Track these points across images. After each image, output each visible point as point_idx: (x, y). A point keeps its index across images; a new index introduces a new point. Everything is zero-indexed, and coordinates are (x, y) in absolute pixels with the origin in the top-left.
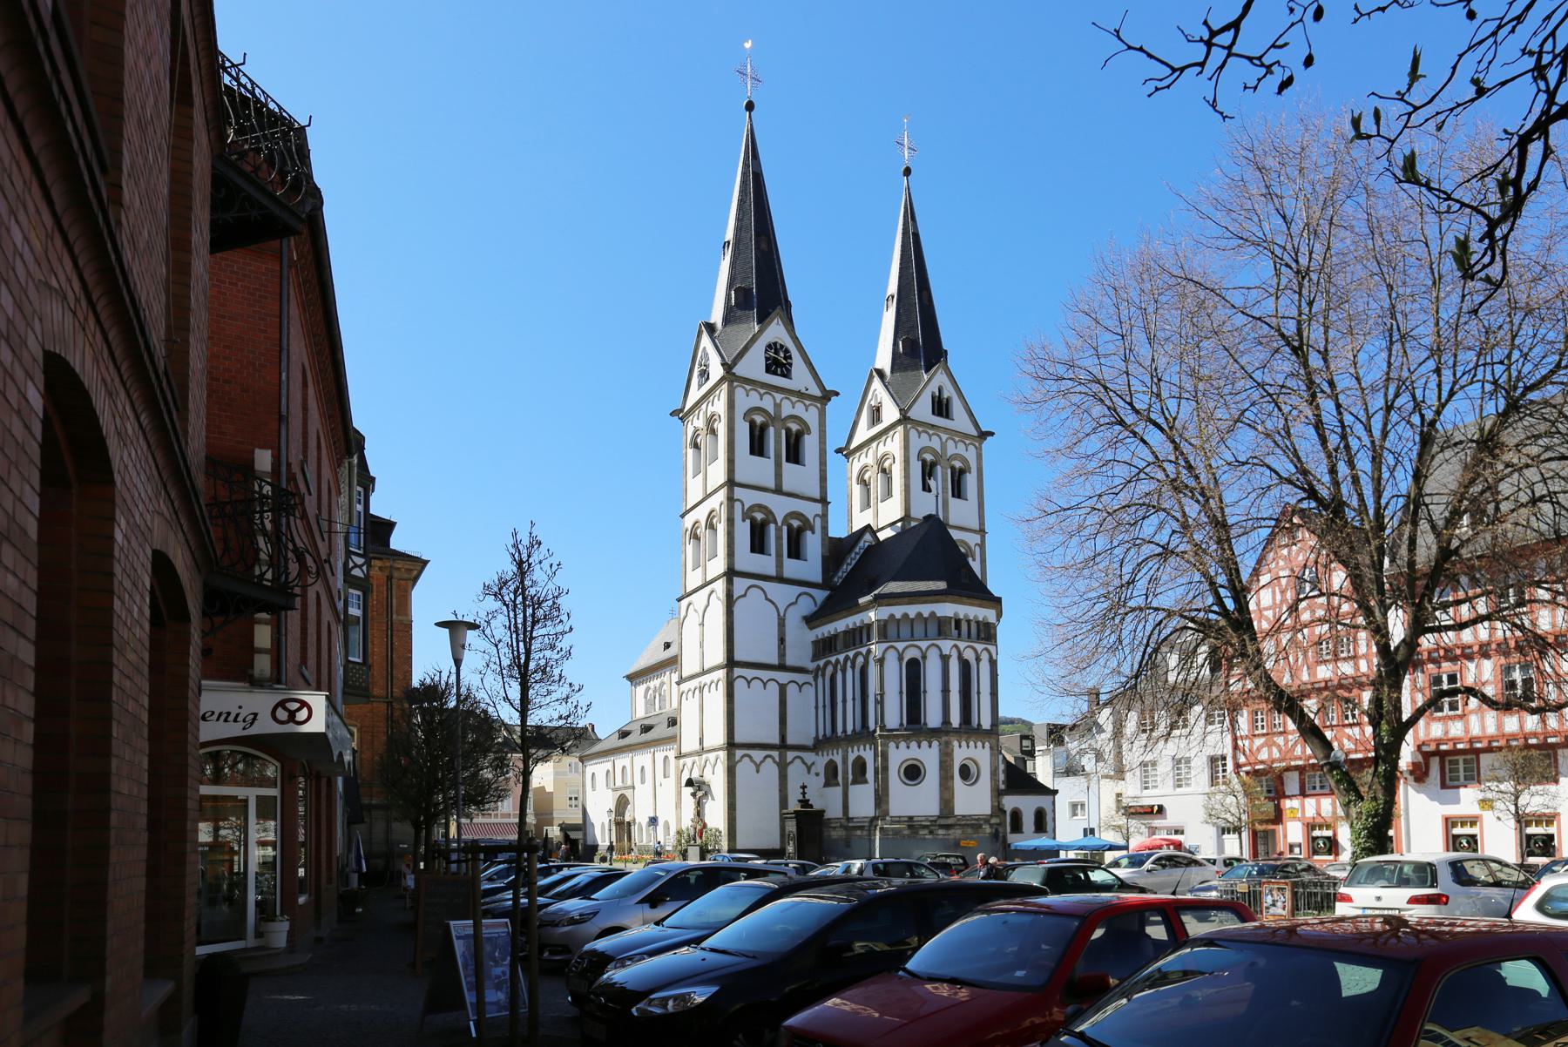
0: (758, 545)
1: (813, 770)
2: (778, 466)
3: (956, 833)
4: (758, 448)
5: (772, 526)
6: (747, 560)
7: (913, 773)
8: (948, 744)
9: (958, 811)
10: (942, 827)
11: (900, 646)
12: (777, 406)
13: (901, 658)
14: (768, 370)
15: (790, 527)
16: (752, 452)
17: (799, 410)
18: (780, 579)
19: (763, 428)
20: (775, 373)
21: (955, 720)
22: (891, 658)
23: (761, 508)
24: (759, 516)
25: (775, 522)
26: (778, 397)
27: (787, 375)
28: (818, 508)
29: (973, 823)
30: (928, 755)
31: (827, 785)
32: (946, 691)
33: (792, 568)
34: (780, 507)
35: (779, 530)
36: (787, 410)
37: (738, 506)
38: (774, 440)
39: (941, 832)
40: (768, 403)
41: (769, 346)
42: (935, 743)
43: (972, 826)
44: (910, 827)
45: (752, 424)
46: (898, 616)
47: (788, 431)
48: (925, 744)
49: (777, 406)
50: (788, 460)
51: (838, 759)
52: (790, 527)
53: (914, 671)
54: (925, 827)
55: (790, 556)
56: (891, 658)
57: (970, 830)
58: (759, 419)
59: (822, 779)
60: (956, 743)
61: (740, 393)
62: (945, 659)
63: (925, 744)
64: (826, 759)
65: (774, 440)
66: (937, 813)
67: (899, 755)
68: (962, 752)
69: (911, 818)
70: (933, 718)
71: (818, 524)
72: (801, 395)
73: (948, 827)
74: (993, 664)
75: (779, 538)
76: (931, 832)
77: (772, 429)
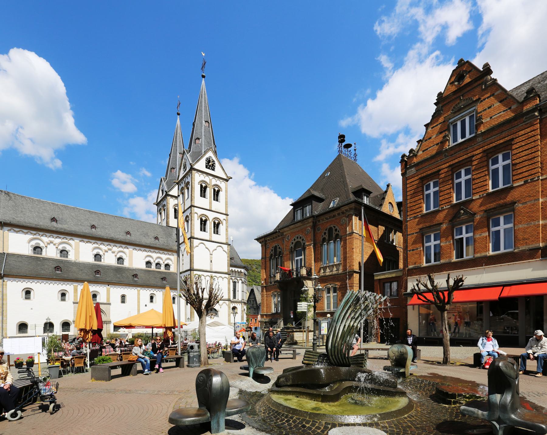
6: (197, 233)
12: (210, 180)
14: (206, 167)
16: (201, 196)
17: (218, 182)
20: (209, 168)
26: (211, 177)
27: (213, 170)
28: (225, 217)
33: (215, 237)
34: (211, 216)
35: (210, 223)
41: (207, 159)
45: (201, 186)
49: (210, 180)
50: (214, 200)
52: (214, 223)
55: (214, 233)
71: (224, 222)
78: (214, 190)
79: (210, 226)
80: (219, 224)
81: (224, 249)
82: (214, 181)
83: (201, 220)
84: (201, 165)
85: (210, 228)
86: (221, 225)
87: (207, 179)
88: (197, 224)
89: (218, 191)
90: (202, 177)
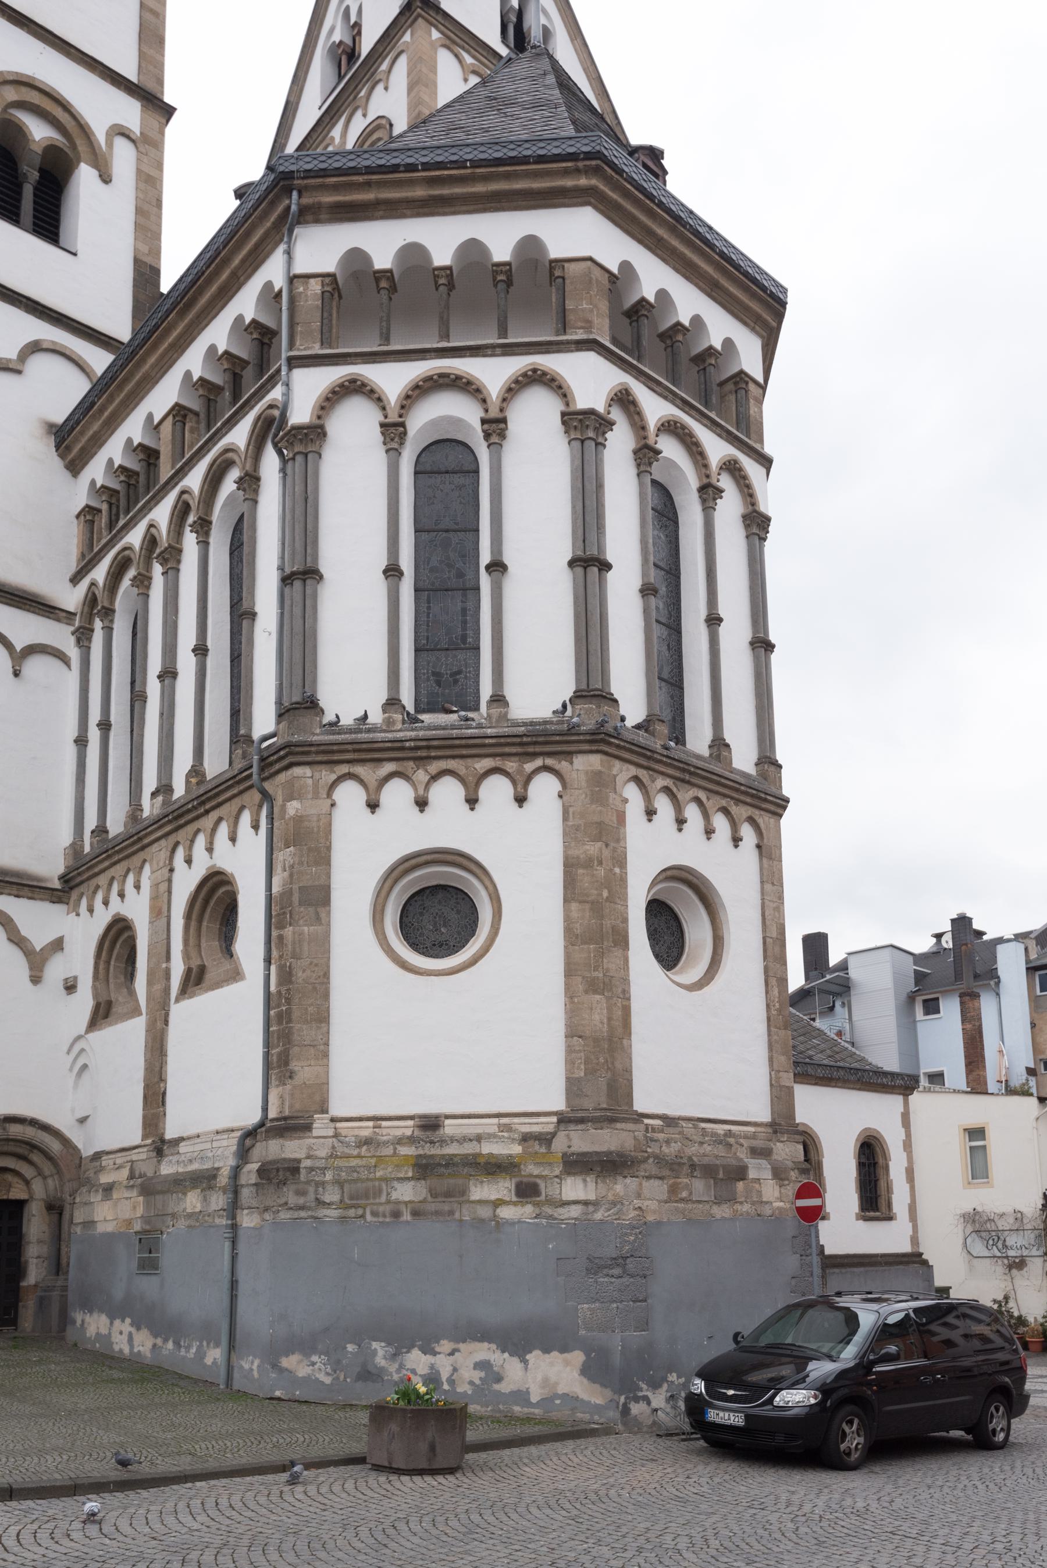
1: (56, 970)
3: (643, 1196)
7: (438, 910)
8: (601, 786)
9: (641, 1104)
10: (578, 1164)
11: (393, 379)
13: (393, 432)
21: (632, 698)
22: (354, 430)
29: (707, 1162)
30: (514, 838)
31: (102, 1014)
32: (589, 563)
39: (575, 1188)
42: (545, 788)
43: (709, 1171)
44: (424, 1168)
46: (383, 260)
48: (497, 791)
51: (136, 907)
53: (447, 492)
54: (495, 1168)
56: (354, 430)
57: (699, 1186)
59: (84, 1001)
60: (632, 792)
62: (584, 428)
63: (497, 791)
64: (103, 918)
66: (553, 1098)
67: (372, 834)
68: (656, 841)
69: (430, 1124)
70: (532, 674)
73: (608, 1166)
74: (757, 524)
76: (527, 1191)
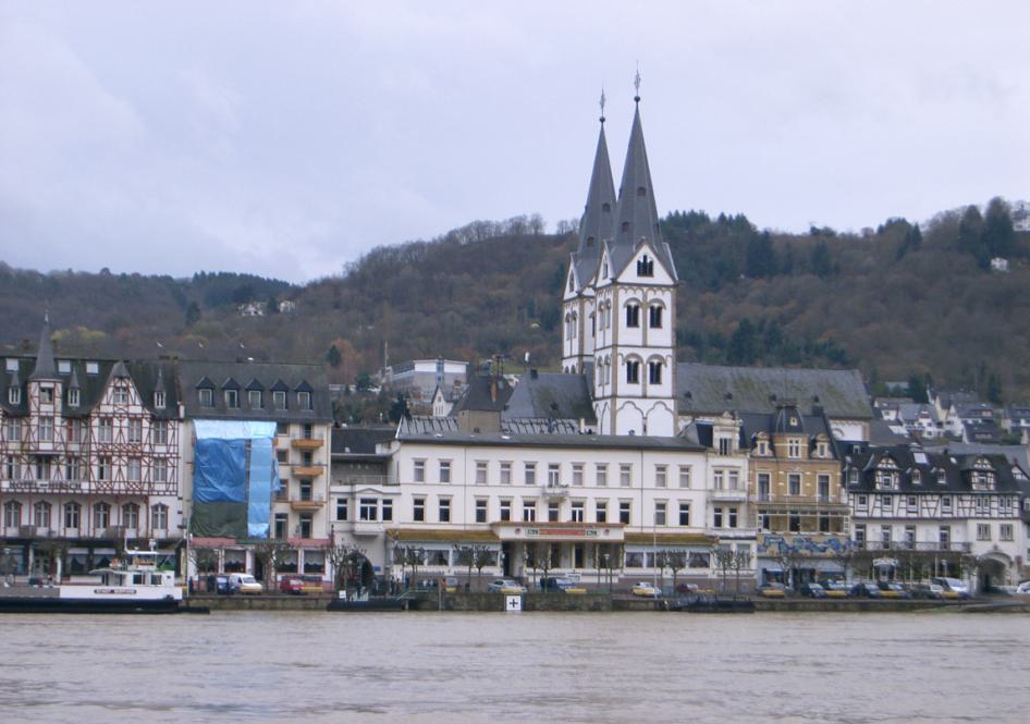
0: (632, 376)
2: (645, 330)
4: (632, 320)
5: (640, 366)
12: (645, 296)
15: (652, 364)
17: (659, 295)
18: (645, 397)
19: (636, 308)
23: (633, 355)
24: (633, 360)
25: (642, 362)
26: (645, 289)
33: (653, 390)
34: (645, 354)
35: (644, 367)
36: (651, 296)
37: (620, 358)
38: (644, 316)
40: (639, 295)
45: (629, 308)
47: (652, 308)
49: (645, 296)
52: (652, 364)
58: (633, 304)
61: (621, 292)
65: (644, 316)
72: (660, 287)
75: (644, 370)
77: (640, 311)
78: (652, 308)
79: (644, 372)
80: (659, 365)
81: (669, 406)
82: (651, 296)
83: (629, 363)
84: (630, 274)
85: (644, 376)
86: (663, 366)
87: (639, 295)
88: (623, 371)
89: (659, 309)
90: (631, 294)
